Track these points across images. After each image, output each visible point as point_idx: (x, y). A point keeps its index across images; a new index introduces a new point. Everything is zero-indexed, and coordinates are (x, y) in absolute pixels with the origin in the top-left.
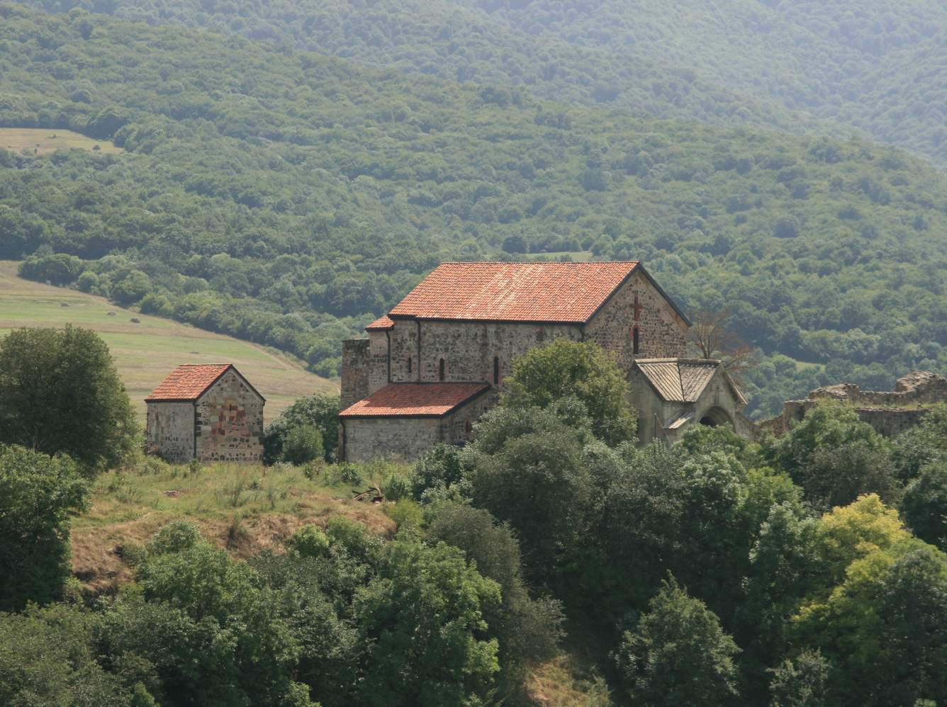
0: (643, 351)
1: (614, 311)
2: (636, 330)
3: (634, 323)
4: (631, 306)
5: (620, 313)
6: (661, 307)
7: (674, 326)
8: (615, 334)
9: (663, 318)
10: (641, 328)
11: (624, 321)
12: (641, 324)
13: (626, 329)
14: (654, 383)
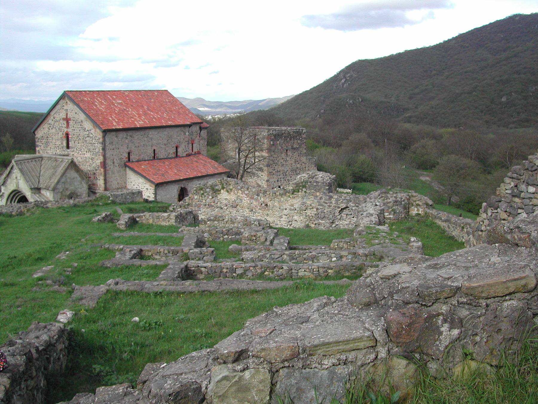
0: (72, 148)
1: (53, 123)
2: (67, 135)
4: (64, 119)
5: (57, 124)
7: (93, 131)
8: (53, 136)
9: (85, 126)
10: (70, 133)
11: (59, 129)
12: (70, 130)
13: (61, 133)
14: (152, 179)
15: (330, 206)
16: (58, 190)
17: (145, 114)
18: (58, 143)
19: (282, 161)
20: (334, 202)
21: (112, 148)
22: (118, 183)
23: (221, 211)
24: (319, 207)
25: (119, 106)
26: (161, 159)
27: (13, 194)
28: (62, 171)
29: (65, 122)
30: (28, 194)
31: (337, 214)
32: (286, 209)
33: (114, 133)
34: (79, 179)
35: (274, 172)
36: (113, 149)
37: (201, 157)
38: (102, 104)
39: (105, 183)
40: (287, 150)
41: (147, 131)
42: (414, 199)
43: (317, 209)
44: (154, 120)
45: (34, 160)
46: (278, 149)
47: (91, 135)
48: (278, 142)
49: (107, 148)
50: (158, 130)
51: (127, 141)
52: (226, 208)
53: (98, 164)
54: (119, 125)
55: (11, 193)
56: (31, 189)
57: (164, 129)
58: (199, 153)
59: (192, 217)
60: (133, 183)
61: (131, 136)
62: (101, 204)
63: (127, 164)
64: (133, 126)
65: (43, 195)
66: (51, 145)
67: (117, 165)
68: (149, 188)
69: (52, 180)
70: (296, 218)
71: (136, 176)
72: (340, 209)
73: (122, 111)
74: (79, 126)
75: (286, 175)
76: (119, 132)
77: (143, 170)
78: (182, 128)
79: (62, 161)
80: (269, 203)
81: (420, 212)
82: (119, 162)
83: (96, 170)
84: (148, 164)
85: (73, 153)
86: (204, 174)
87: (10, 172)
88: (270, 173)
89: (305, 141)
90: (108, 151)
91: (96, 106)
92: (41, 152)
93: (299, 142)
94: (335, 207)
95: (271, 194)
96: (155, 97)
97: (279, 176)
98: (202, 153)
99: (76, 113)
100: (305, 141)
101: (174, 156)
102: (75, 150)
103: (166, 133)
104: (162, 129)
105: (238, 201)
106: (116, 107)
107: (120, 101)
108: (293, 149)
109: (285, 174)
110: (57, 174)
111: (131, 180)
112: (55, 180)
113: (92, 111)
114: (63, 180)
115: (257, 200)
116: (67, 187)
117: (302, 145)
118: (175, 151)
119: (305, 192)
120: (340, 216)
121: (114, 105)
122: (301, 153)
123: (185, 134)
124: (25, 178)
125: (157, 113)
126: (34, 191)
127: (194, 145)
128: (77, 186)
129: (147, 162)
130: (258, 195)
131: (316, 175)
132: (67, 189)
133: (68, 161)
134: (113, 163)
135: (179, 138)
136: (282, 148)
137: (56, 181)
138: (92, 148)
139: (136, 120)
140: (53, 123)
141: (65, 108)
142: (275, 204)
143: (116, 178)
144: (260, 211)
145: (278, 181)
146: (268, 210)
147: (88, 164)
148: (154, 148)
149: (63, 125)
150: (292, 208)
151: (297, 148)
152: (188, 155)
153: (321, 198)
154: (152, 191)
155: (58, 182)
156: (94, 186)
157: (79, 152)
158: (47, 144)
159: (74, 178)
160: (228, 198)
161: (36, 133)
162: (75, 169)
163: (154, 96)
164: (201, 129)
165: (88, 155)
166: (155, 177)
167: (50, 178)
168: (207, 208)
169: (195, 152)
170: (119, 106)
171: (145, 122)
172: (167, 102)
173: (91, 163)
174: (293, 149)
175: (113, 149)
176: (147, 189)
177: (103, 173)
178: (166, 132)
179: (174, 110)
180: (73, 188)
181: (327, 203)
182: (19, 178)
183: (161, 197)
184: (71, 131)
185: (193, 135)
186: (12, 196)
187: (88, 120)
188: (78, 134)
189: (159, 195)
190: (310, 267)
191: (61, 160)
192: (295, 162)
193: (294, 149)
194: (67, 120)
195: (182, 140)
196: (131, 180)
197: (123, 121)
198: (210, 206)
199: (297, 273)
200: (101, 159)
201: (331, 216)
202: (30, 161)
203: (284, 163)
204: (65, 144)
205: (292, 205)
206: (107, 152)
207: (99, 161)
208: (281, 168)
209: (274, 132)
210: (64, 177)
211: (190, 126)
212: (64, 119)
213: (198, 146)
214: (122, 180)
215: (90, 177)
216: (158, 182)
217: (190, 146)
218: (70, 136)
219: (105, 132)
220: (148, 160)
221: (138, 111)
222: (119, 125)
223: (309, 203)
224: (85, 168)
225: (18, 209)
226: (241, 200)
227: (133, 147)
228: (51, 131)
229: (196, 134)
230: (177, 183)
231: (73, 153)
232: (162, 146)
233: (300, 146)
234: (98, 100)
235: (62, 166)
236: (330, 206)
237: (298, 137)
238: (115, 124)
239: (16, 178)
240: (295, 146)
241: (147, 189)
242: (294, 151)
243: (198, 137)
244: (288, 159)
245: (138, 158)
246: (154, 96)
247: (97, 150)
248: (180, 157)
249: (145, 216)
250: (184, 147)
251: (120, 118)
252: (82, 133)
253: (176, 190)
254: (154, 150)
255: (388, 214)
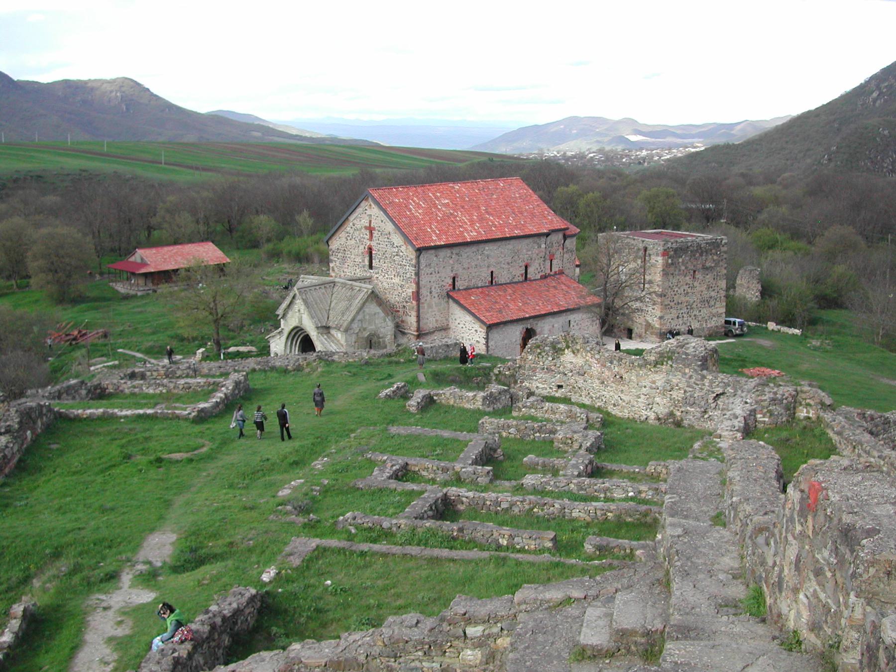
1: (351, 232)
3: (368, 243)
4: (366, 228)
6: (391, 231)
7: (403, 248)
12: (373, 243)
13: (362, 247)
14: (482, 318)
15: (702, 389)
16: (352, 331)
17: (481, 219)
18: (358, 260)
19: (686, 287)
20: (707, 384)
21: (429, 272)
22: (437, 321)
23: (565, 378)
24: (687, 389)
25: (444, 209)
26: (502, 284)
27: (295, 331)
28: (359, 305)
29: (368, 232)
30: (313, 334)
31: (711, 401)
32: (645, 387)
33: (433, 251)
34: (382, 315)
35: (672, 304)
36: (431, 274)
37: (563, 278)
38: (418, 206)
39: (418, 321)
40: (694, 272)
41: (482, 246)
42: (804, 396)
43: (685, 391)
44: (493, 229)
45: (323, 287)
46: (680, 270)
47: (401, 254)
48: (680, 260)
49: (422, 272)
50: (499, 243)
51: (451, 262)
52: (570, 374)
53: (409, 294)
54: (440, 239)
55: (292, 330)
56: (317, 328)
57: (508, 242)
58: (561, 273)
59: (508, 397)
60: (458, 321)
61: (457, 254)
62: (402, 360)
63: (451, 294)
64: (460, 241)
65: (333, 336)
66: (349, 262)
67: (436, 295)
68: (480, 329)
69: (345, 317)
70: (657, 399)
71: (462, 312)
72: (715, 395)
73: (447, 217)
74: (386, 240)
75: (692, 308)
76: (439, 250)
77: (473, 303)
78: (536, 239)
79: (359, 290)
80: (625, 376)
81: (811, 415)
82: (439, 291)
83: (407, 302)
84: (482, 293)
85: (377, 276)
86: (562, 309)
87: (291, 303)
88: (666, 305)
89: (725, 256)
90: (423, 277)
91: (410, 210)
92: (336, 269)
93: (715, 257)
94: (709, 391)
95: (627, 363)
96: (499, 190)
97: (681, 309)
98: (567, 272)
99: (382, 221)
100: (725, 256)
101: (521, 279)
102: (380, 271)
103: (510, 247)
104: (503, 242)
105: (586, 367)
106: (439, 210)
107: (447, 201)
108: (705, 268)
109: (690, 307)
110: (352, 308)
111: (456, 317)
112: (348, 317)
113: (404, 219)
114: (360, 317)
115: (609, 369)
116: (364, 326)
117: (721, 263)
118: (524, 271)
119: (671, 366)
120: (715, 404)
121: (436, 207)
122: (717, 275)
123: (540, 247)
124: (310, 312)
125: (499, 217)
126: (321, 331)
127: (554, 262)
128: (380, 325)
129: (480, 290)
130: (611, 363)
131: (688, 344)
132: (365, 329)
133: (367, 292)
134: (431, 293)
135: (530, 253)
136: (686, 268)
137: (349, 319)
138: (401, 271)
139: (466, 230)
140: (351, 232)
141: (368, 212)
142: (633, 378)
143: (433, 313)
144: (613, 385)
145: (678, 317)
146: (623, 385)
147: (396, 293)
148: (491, 269)
149: (365, 236)
150: (654, 385)
151: (712, 267)
152: (544, 277)
153: (691, 377)
154: (483, 335)
155: (353, 320)
156: (403, 324)
157: (385, 276)
158: (344, 259)
159: (375, 314)
160: (573, 361)
161: (330, 243)
162: (377, 301)
163: (497, 189)
164: (565, 237)
165: (397, 280)
166: (488, 314)
167: (343, 314)
168: (545, 373)
169: (556, 272)
170: (444, 209)
171: (479, 233)
172: (516, 197)
173: (401, 291)
174: (705, 268)
175: (431, 274)
176: (476, 331)
177: (415, 307)
178: (511, 245)
179: (526, 210)
180: (373, 327)
181: (698, 385)
182: (302, 311)
183: (496, 343)
184: (375, 244)
185: (552, 247)
186: (293, 333)
187: (397, 232)
188: (384, 250)
189: (492, 340)
190: (586, 508)
191: (358, 288)
192: (709, 288)
193: (707, 269)
194: (371, 229)
195: (535, 255)
196: (456, 317)
197: (446, 233)
198: (549, 370)
199: (571, 513)
200: (414, 286)
201: (703, 403)
202: (317, 287)
203: (689, 290)
204: (367, 263)
205: (654, 382)
206: (422, 277)
207: (411, 291)
208: (683, 299)
209: (674, 246)
210: (361, 313)
211: (547, 235)
212: (366, 228)
213: (560, 262)
214: (442, 316)
215: (399, 311)
216: (491, 322)
217: (548, 263)
218: (373, 252)
219: (420, 251)
220: (482, 287)
221: (471, 215)
222: (440, 239)
223: (675, 381)
224: (393, 298)
225: (296, 362)
226: (589, 366)
227: (461, 270)
228: (349, 242)
229: (557, 244)
230: (520, 323)
231: (377, 276)
232: (504, 266)
233: (717, 265)
234: (414, 202)
235: (359, 298)
236: (702, 389)
237: (713, 251)
238: (434, 238)
239: (299, 311)
240: (708, 264)
241: (476, 331)
242: (707, 272)
243: (561, 250)
244: (696, 284)
245: (466, 284)
246: (497, 189)
247: (408, 275)
248: (530, 280)
249: (444, 394)
250: (537, 266)
251: (444, 228)
252: (390, 250)
253: (518, 333)
254: (492, 272)
255: (761, 416)
